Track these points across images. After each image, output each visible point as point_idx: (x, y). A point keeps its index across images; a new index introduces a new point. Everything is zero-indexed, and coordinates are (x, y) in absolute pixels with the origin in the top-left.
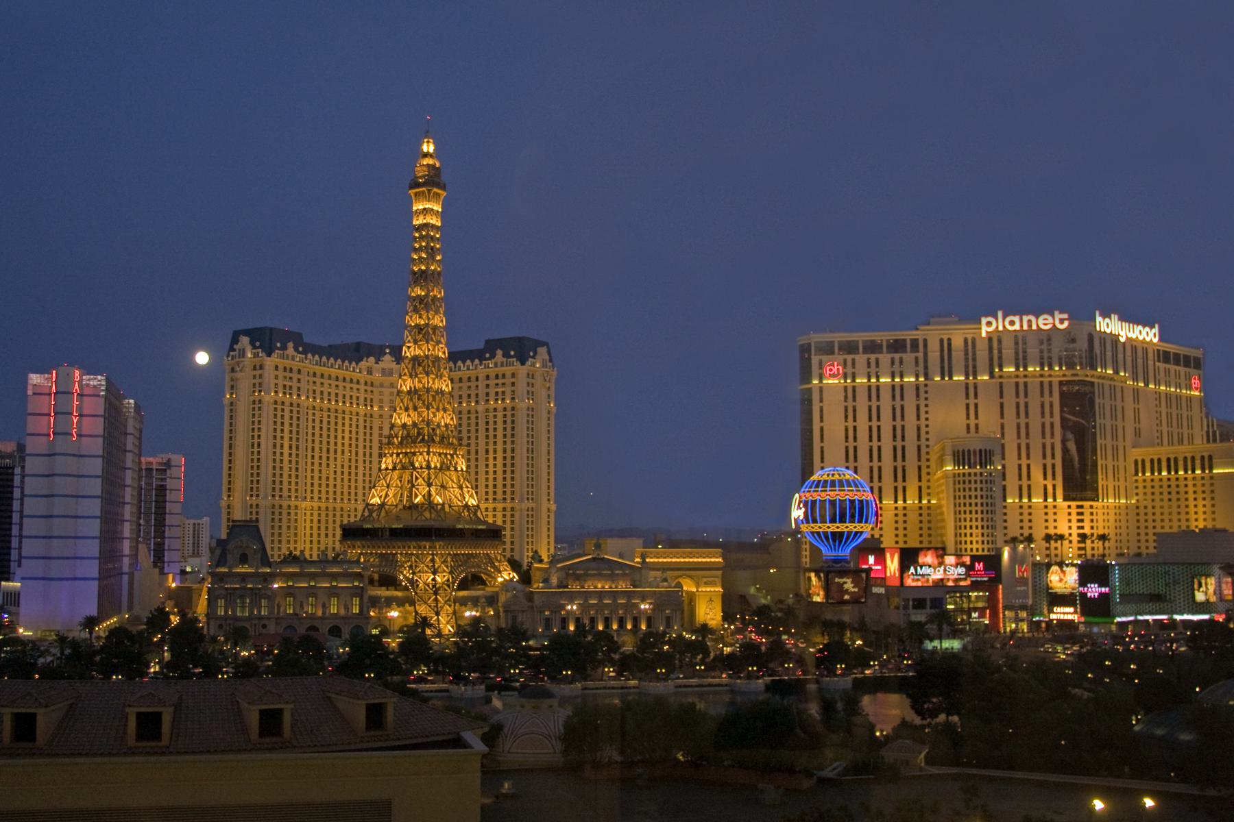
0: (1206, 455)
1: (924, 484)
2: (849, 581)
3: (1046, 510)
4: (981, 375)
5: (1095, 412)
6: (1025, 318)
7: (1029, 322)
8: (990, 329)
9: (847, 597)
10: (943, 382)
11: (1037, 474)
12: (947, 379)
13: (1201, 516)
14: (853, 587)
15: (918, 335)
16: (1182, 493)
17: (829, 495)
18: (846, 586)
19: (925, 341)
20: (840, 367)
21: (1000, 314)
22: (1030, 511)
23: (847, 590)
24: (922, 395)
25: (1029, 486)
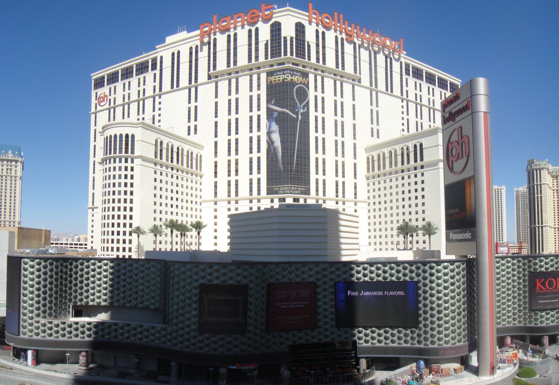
5: (308, 102)
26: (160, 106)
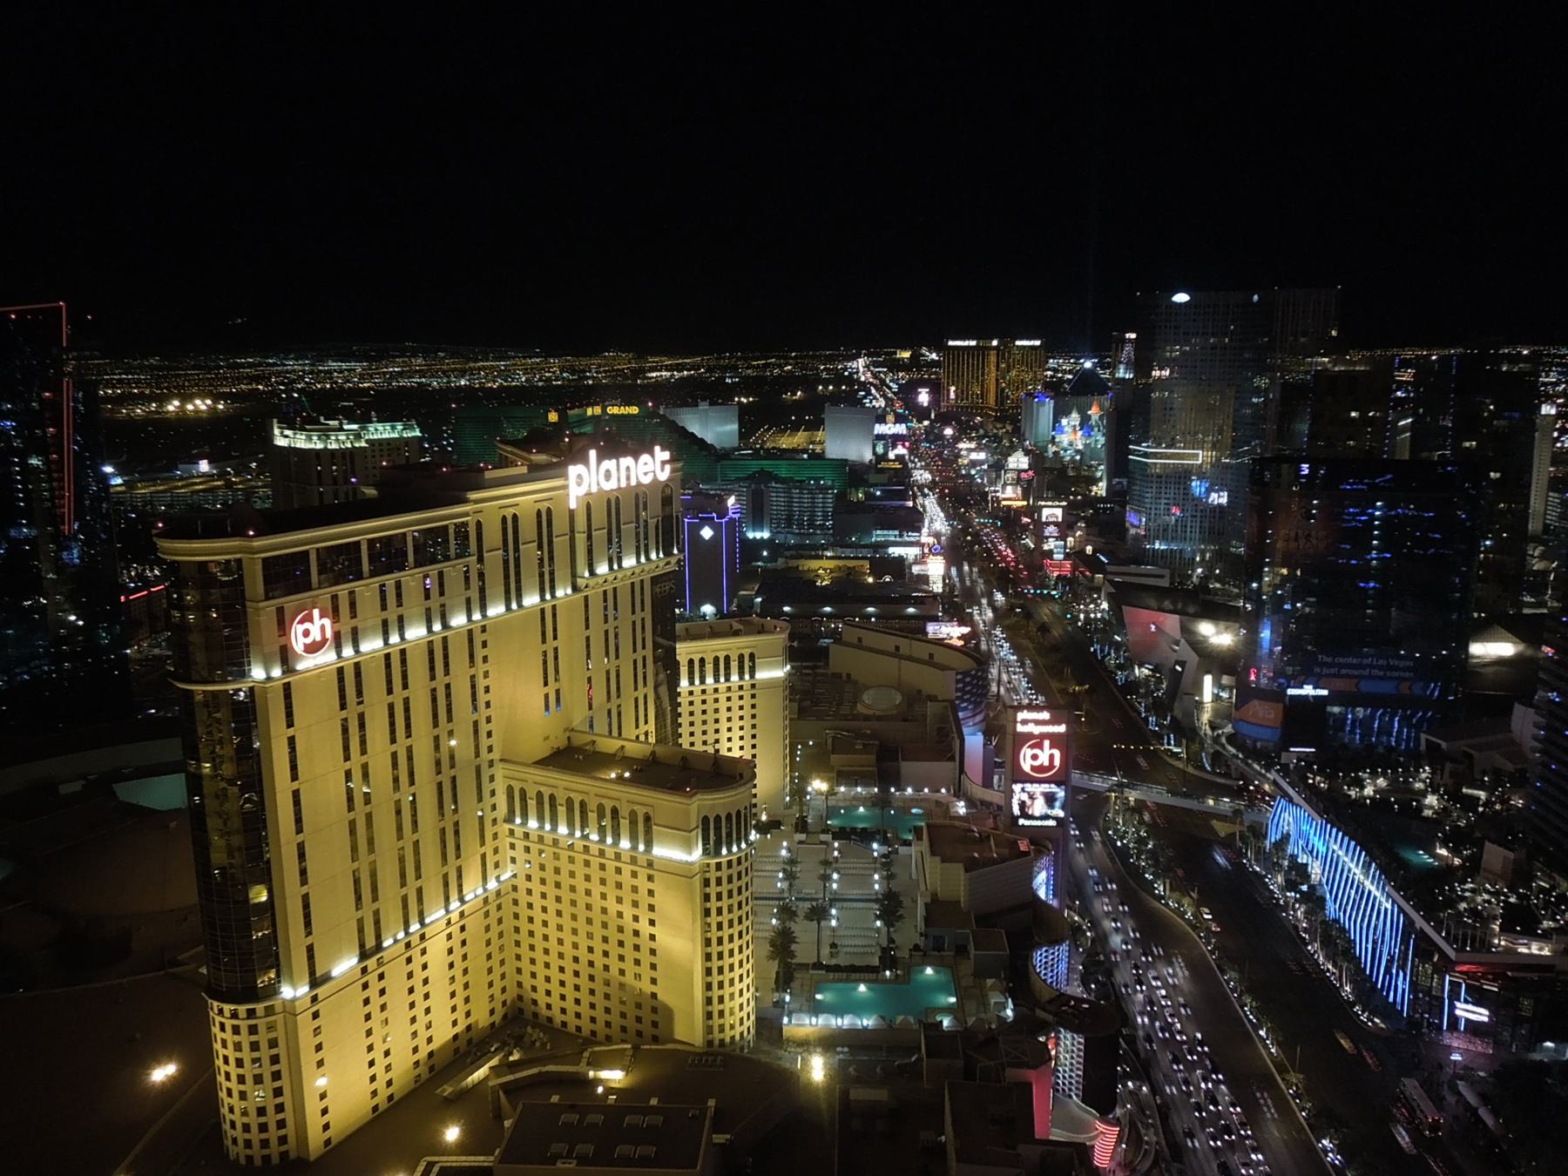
0: (746, 652)
1: (488, 849)
8: (582, 491)
13: (736, 744)
15: (467, 514)
16: (710, 712)
20: (327, 622)
21: (593, 454)
26: (485, 652)
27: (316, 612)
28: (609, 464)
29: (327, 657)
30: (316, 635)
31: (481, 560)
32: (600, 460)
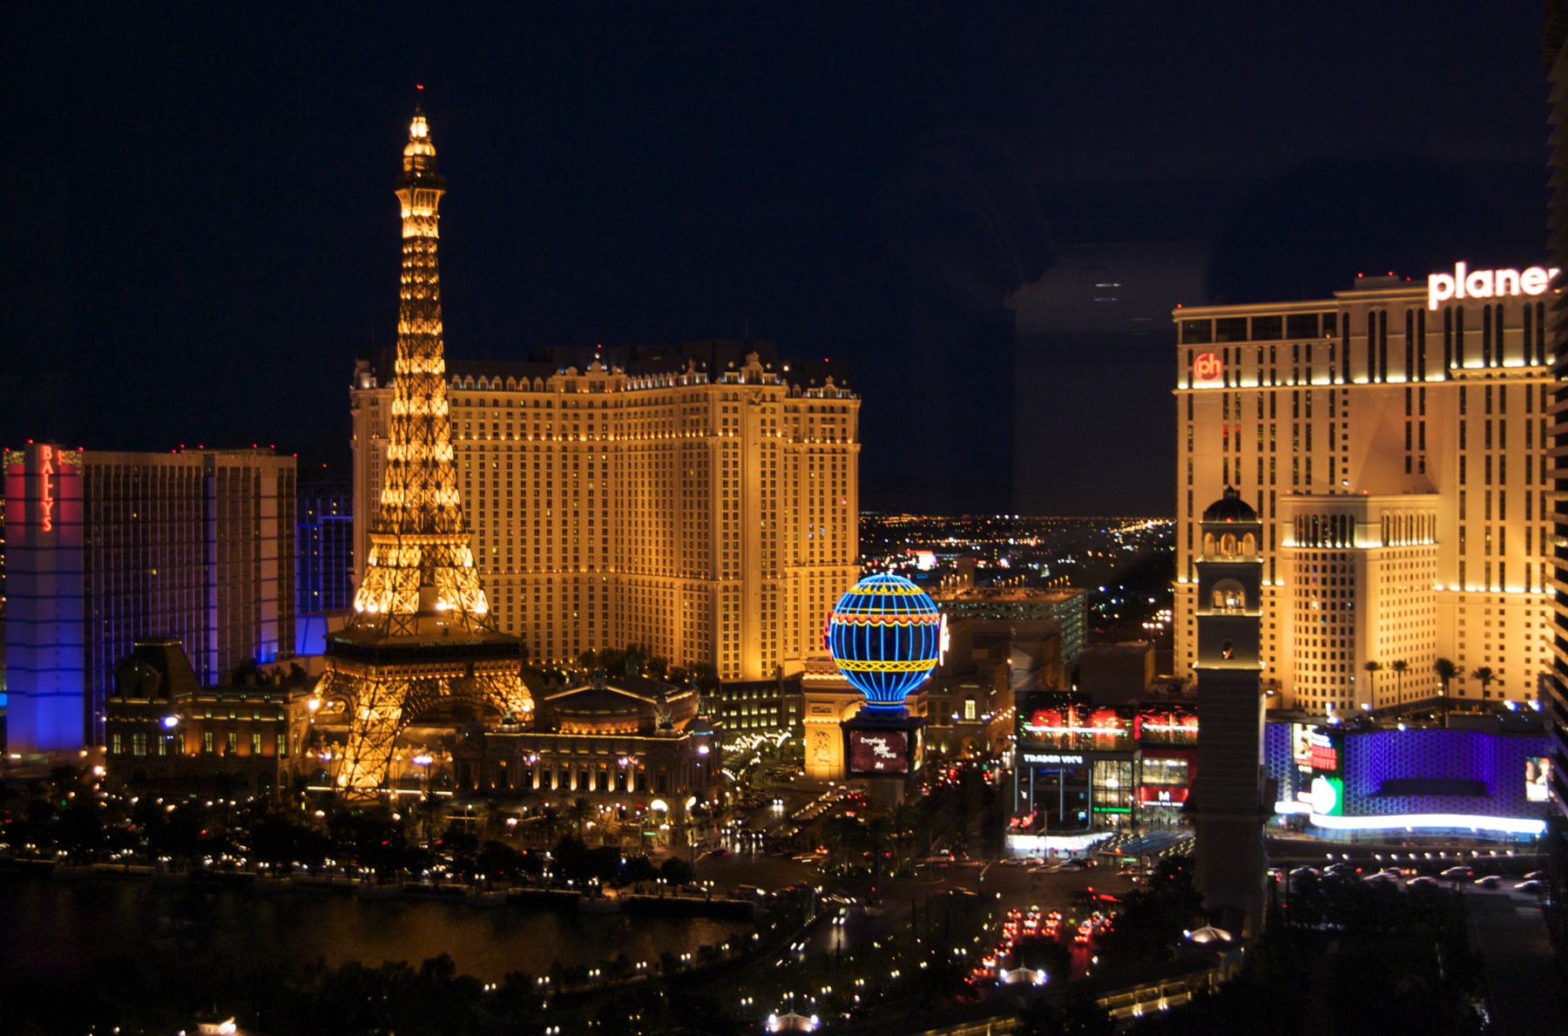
2: (882, 742)
3: (1528, 607)
4: (1432, 373)
6: (1502, 274)
7: (1508, 280)
8: (1445, 296)
9: (879, 765)
10: (1372, 386)
11: (1515, 542)
12: (1377, 380)
14: (889, 752)
17: (869, 619)
18: (877, 750)
19: (1346, 317)
20: (1218, 363)
21: (1460, 267)
22: (1502, 606)
23: (879, 755)
24: (1339, 409)
25: (1502, 565)
27: (1211, 356)
28: (1477, 275)
29: (1218, 384)
30: (1210, 369)
31: (1346, 342)
32: (1469, 271)
